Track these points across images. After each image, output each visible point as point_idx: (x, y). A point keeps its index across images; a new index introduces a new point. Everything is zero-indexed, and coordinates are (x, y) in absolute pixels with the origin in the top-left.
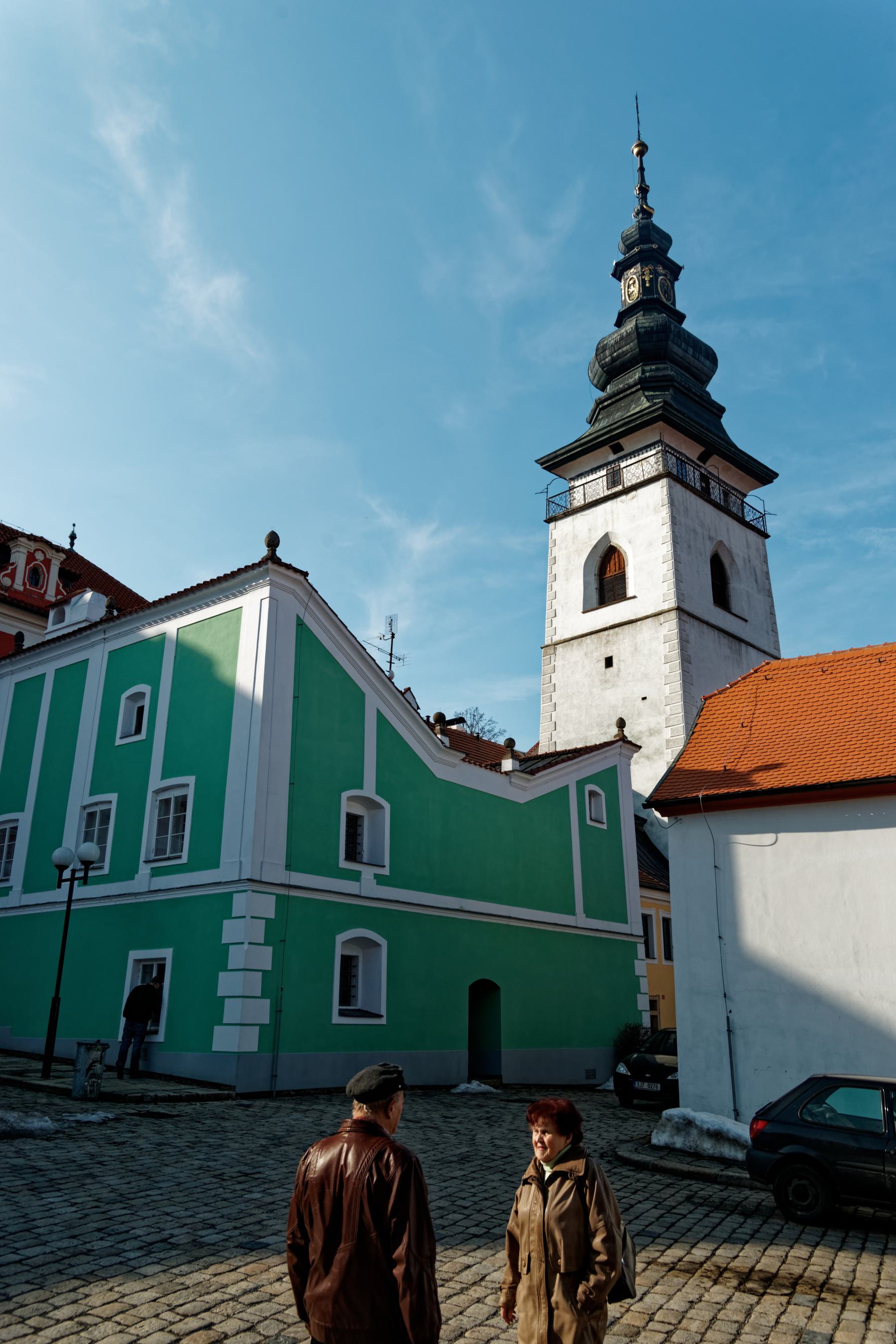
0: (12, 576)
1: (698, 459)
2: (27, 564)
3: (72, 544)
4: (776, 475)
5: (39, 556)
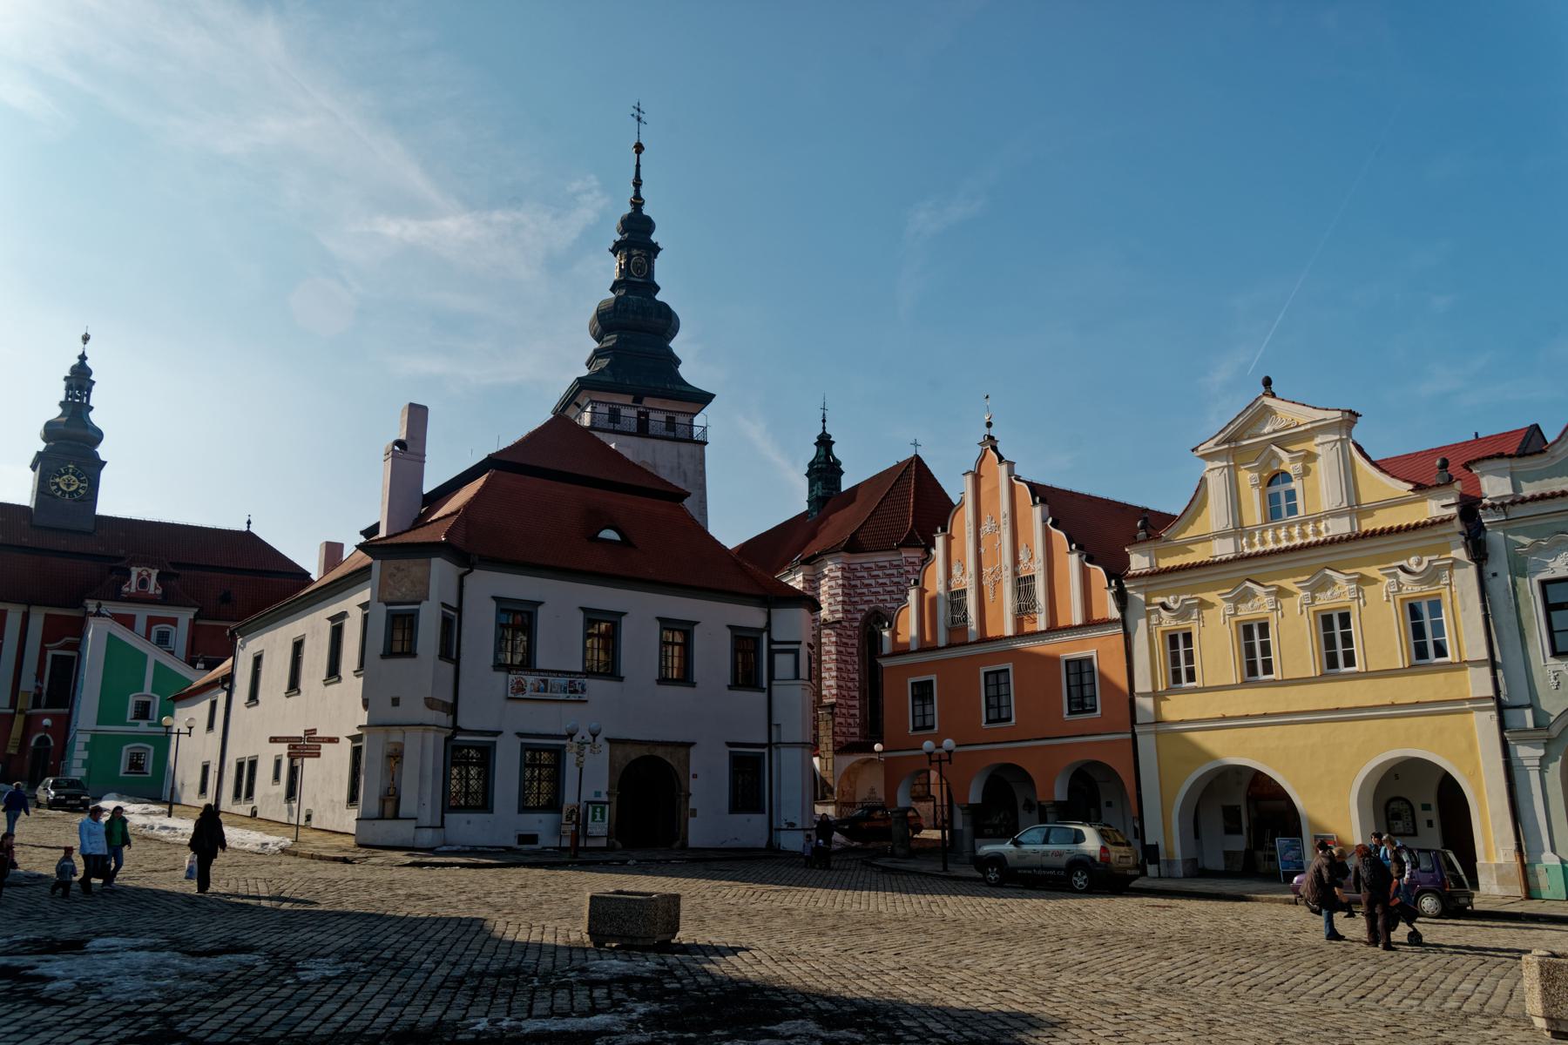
0: (130, 586)
1: (633, 402)
2: (138, 578)
3: (249, 527)
4: (713, 396)
5: (145, 573)
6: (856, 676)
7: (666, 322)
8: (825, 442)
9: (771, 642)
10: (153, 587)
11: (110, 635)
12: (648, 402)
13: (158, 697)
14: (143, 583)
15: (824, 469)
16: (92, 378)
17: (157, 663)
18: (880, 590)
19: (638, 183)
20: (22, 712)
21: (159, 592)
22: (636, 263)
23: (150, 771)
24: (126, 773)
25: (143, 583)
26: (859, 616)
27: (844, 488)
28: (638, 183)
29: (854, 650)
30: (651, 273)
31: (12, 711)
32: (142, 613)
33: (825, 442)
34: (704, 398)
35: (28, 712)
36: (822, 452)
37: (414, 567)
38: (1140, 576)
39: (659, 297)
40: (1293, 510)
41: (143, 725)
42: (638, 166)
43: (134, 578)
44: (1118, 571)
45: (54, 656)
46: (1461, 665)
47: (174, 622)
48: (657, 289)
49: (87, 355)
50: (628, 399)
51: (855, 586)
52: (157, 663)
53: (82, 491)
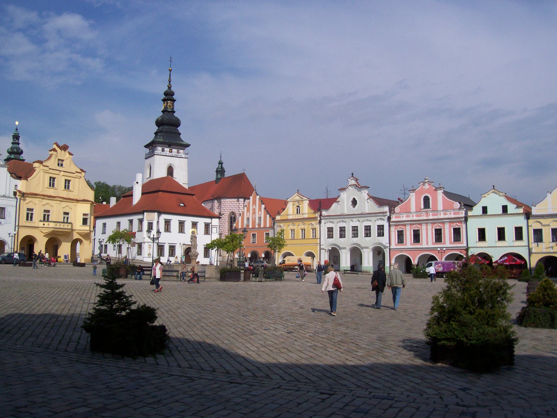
4: (190, 145)
6: (227, 227)
7: (177, 123)
8: (221, 163)
9: (212, 225)
12: (172, 146)
15: (220, 171)
18: (234, 207)
19: (170, 81)
22: (169, 105)
26: (228, 213)
27: (225, 176)
28: (170, 81)
29: (227, 221)
30: (173, 108)
33: (221, 163)
34: (188, 146)
36: (220, 166)
37: (152, 214)
38: (277, 220)
39: (175, 114)
40: (299, 213)
42: (170, 75)
44: (274, 219)
46: (317, 238)
48: (175, 112)
50: (167, 146)
51: (228, 206)
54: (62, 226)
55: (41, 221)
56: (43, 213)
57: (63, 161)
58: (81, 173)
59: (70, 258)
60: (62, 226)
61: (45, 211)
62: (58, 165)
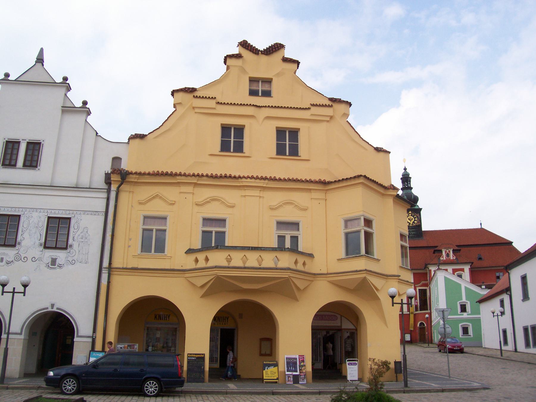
0: (443, 257)
2: (445, 253)
3: (481, 226)
10: (452, 257)
11: (445, 277)
13: (469, 302)
14: (448, 255)
16: (410, 176)
17: (465, 287)
20: (412, 313)
21: (454, 258)
23: (472, 335)
24: (462, 336)
25: (448, 255)
31: (409, 313)
32: (450, 269)
35: (414, 313)
41: (465, 315)
43: (444, 253)
45: (419, 290)
47: (463, 270)
49: (406, 168)
52: (465, 287)
53: (416, 222)
54: (268, 260)
55: (190, 251)
56: (199, 228)
57: (269, 81)
58: (332, 106)
59: (309, 368)
60: (268, 260)
61: (207, 221)
62: (253, 93)
